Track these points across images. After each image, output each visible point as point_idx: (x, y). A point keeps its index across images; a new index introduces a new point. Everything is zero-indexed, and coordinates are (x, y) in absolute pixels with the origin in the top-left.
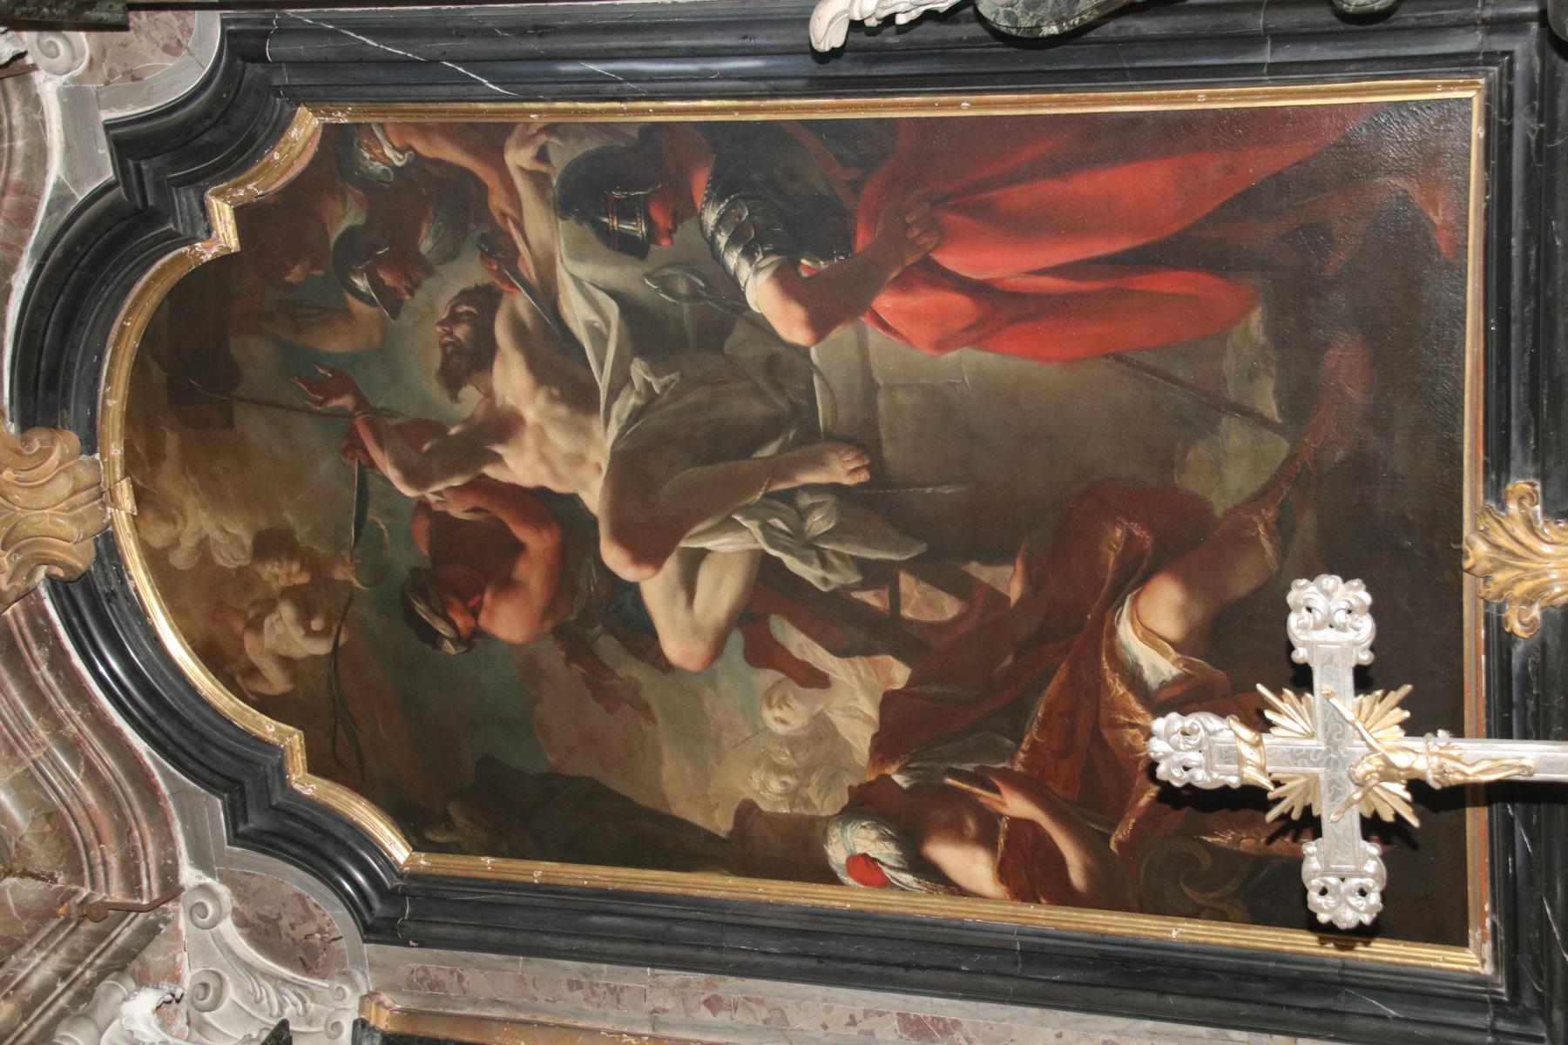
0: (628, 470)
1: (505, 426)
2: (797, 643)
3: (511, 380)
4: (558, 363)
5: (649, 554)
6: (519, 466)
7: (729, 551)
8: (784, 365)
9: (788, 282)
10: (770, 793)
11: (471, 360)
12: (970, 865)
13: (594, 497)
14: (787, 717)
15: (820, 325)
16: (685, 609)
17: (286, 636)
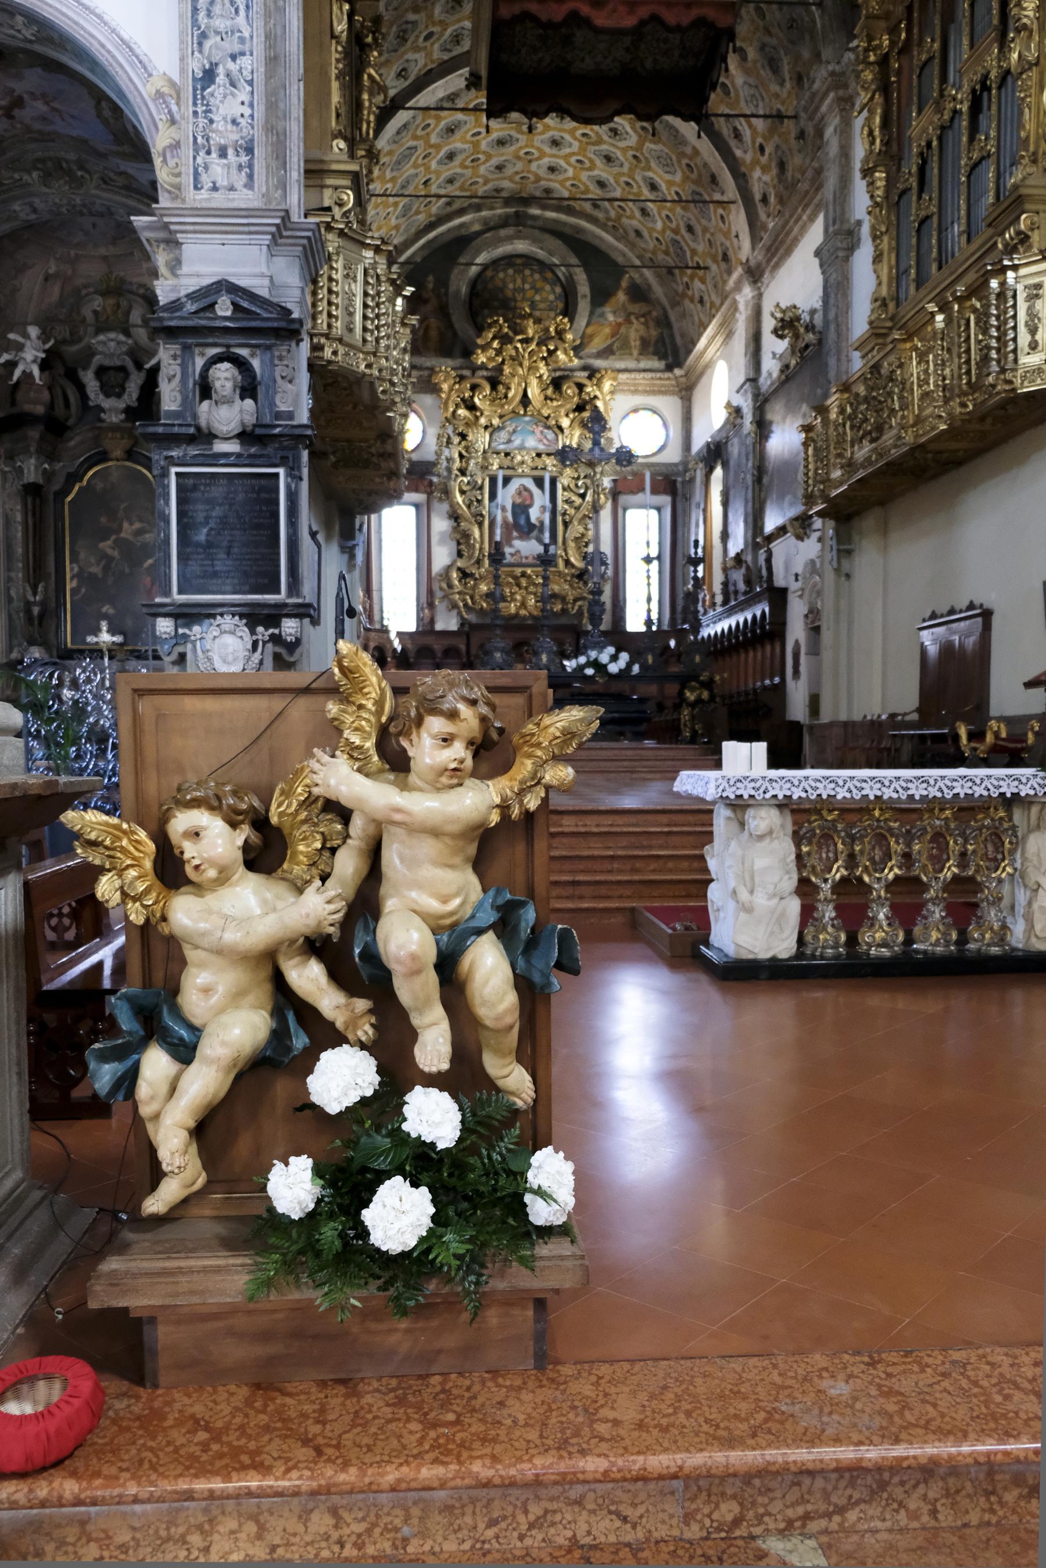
0: (126, 540)
1: (131, 524)
2: (103, 563)
3: (137, 525)
4: (139, 533)
5: (115, 542)
6: (126, 525)
7: (116, 554)
8: (141, 564)
9: (151, 565)
10: (82, 556)
11: (141, 520)
12: (74, 584)
13: (123, 535)
14: (93, 560)
15: (147, 569)
16: (106, 546)
17: (100, 486)
